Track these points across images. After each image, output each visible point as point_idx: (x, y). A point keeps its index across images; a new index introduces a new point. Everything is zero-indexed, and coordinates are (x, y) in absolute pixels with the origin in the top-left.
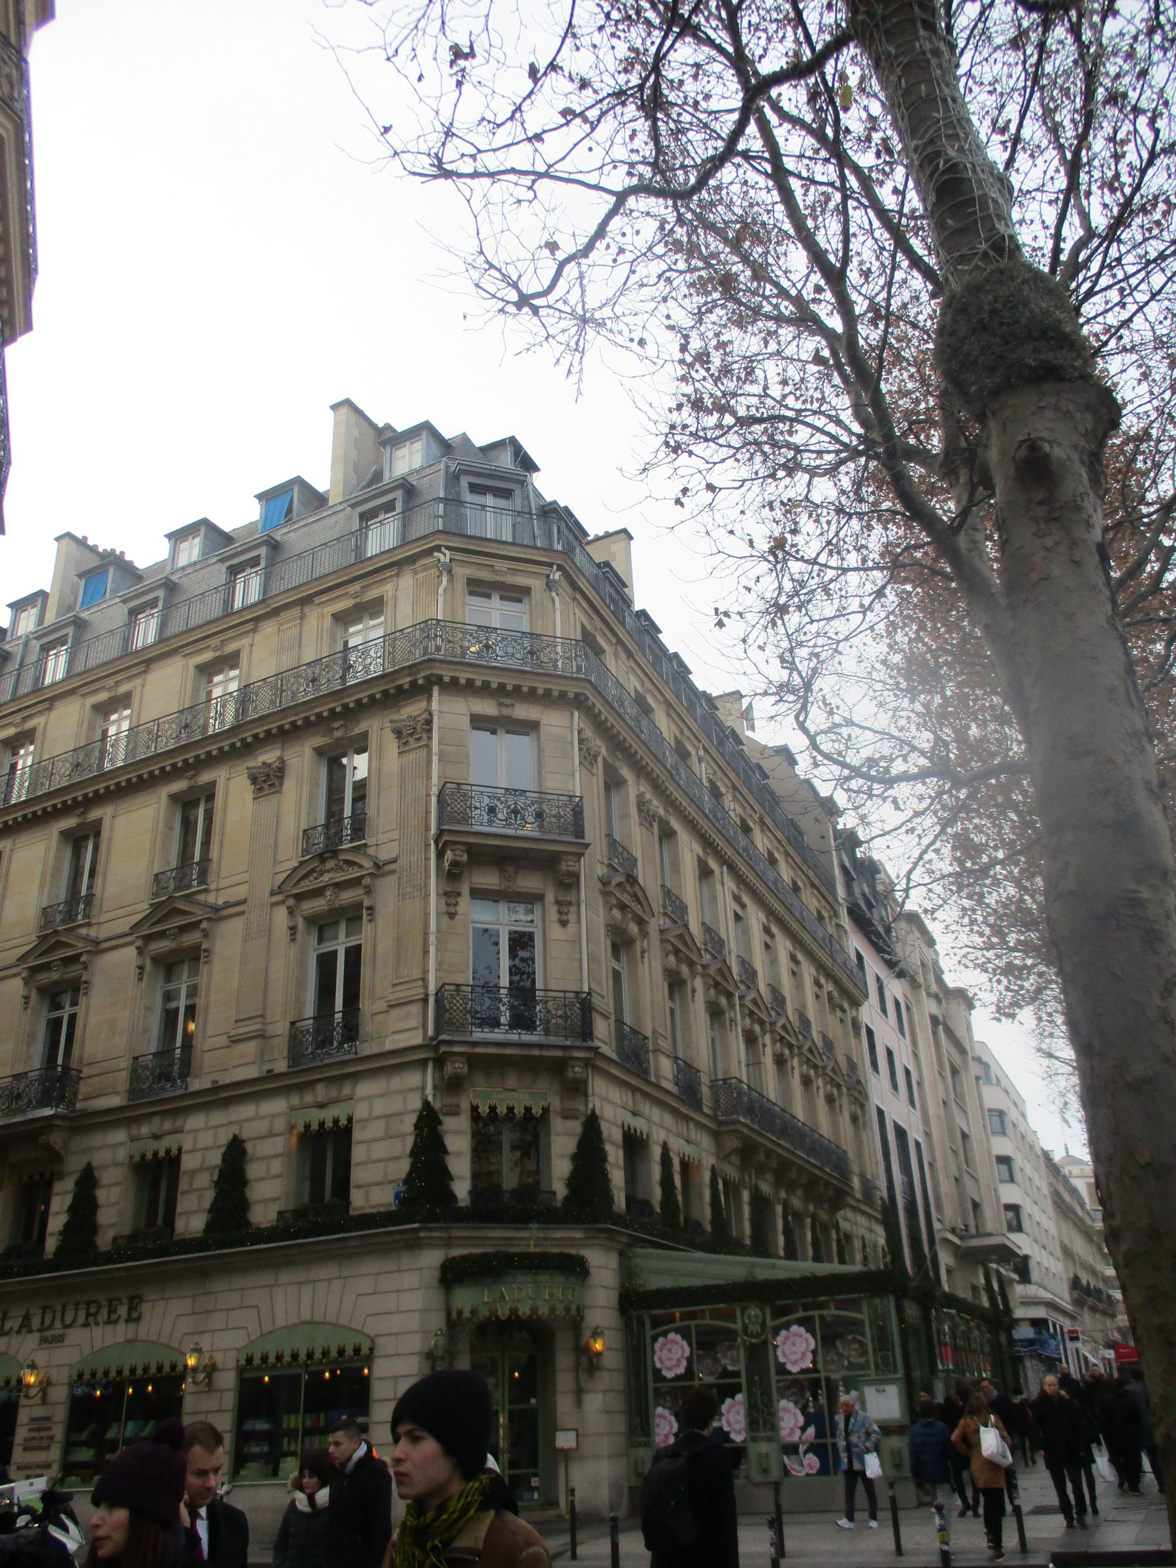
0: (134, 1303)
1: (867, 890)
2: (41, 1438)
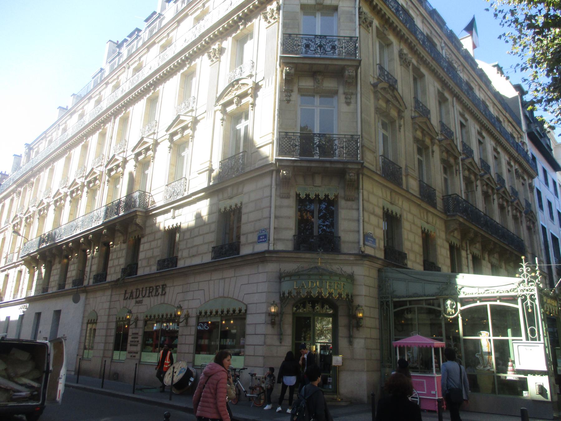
0: (164, 287)
1: (538, 129)
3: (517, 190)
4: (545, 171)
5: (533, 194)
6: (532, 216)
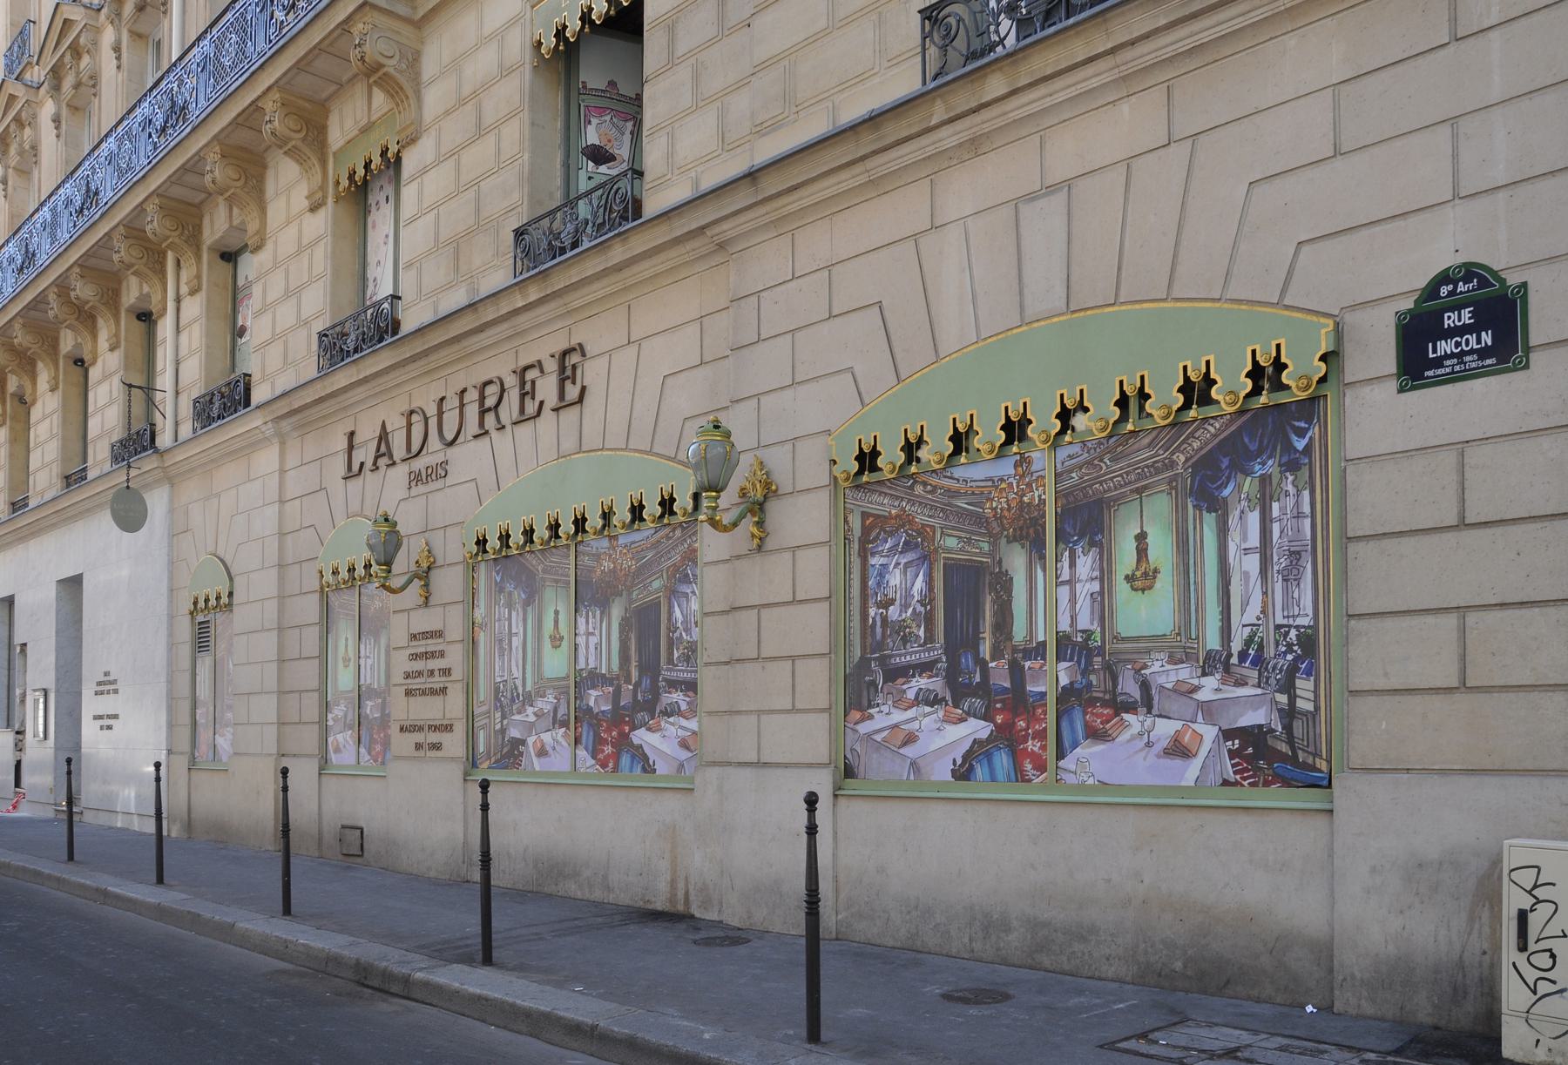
2: (432, 673)
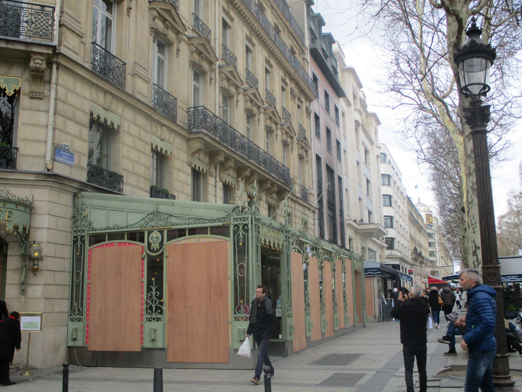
1: (324, 46)
3: (290, 112)
4: (327, 95)
5: (310, 120)
6: (306, 144)
